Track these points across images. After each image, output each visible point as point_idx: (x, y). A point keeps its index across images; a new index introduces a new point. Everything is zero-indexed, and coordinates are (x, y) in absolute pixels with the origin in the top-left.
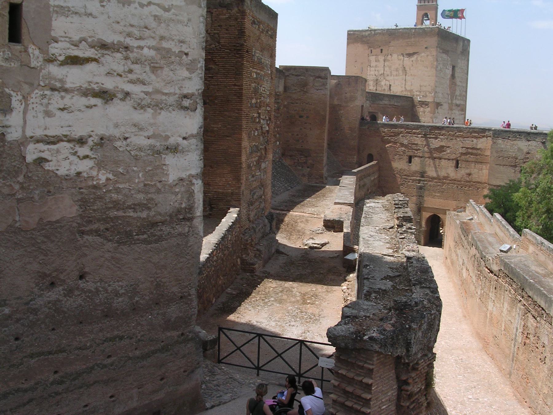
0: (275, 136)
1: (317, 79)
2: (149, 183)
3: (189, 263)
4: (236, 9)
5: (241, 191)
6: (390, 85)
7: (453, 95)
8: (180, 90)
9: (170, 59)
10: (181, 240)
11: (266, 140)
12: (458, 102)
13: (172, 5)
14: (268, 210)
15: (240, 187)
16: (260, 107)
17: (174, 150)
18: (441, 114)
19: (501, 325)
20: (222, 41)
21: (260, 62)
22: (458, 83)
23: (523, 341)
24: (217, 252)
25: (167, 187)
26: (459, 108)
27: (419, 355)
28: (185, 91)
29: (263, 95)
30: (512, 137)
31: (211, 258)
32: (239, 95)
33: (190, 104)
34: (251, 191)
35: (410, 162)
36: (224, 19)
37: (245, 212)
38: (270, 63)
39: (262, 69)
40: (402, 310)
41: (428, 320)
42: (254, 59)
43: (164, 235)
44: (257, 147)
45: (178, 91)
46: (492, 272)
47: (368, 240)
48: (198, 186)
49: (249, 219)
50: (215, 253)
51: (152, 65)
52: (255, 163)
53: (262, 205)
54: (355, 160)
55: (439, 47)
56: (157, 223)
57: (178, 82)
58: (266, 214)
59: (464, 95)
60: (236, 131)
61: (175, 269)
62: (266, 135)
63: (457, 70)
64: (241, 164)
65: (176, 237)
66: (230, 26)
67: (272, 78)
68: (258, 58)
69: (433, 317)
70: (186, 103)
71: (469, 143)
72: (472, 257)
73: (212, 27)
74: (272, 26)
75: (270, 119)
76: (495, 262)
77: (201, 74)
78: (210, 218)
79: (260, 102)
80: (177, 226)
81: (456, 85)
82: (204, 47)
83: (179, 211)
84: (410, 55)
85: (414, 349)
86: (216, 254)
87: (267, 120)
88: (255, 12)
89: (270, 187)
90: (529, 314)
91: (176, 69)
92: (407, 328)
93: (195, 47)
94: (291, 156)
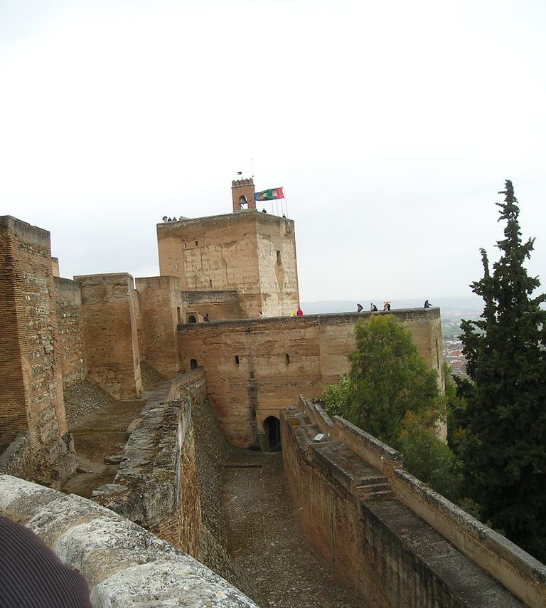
0: (76, 353)
7: (281, 284)
12: (288, 291)
26: (290, 297)
27: (158, 520)
35: (237, 362)
44: (41, 368)
49: (40, 440)
53: (56, 427)
55: (259, 233)
58: (61, 435)
64: (23, 387)
71: (296, 334)
74: (44, 245)
75: (54, 339)
81: (283, 271)
84: (228, 245)
85: (150, 515)
89: (63, 406)
94: (98, 373)
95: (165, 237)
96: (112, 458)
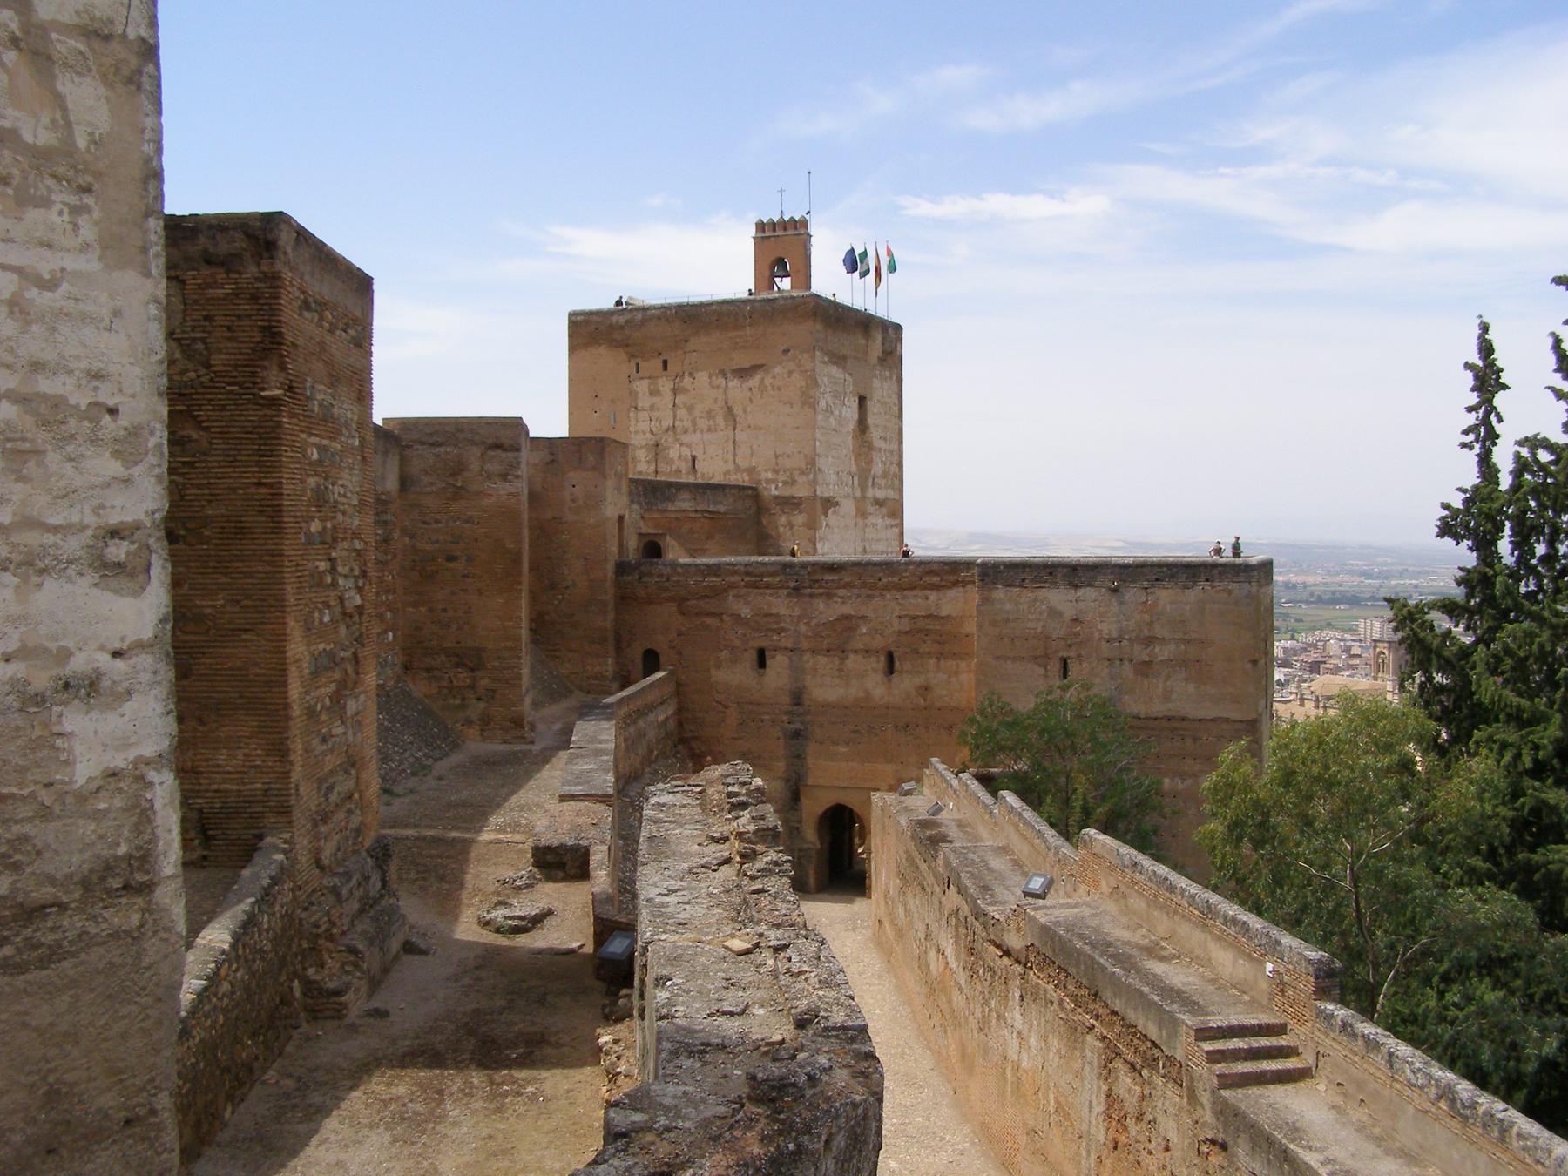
0: (381, 617)
1: (491, 453)
2: (15, 790)
3: (148, 1017)
4: (252, 270)
5: (293, 786)
6: (694, 459)
7: (864, 477)
8: (98, 515)
9: (63, 427)
10: (119, 952)
11: (357, 634)
12: (880, 494)
13: (63, 270)
14: (372, 833)
15: (286, 775)
16: (335, 540)
17: (85, 689)
18: (836, 530)
19: (1046, 1098)
20: (217, 360)
21: (327, 418)
22: (878, 443)
23: (1110, 1138)
24: (230, 966)
25: (69, 800)
26: (884, 510)
28: (114, 519)
29: (341, 507)
30: (1032, 581)
31: (213, 989)
32: (275, 513)
33: (128, 553)
34: (320, 781)
35: (762, 662)
36: (219, 299)
37: (305, 842)
38: (356, 418)
39: (335, 435)
40: (773, 1100)
41: (847, 1123)
42: (310, 407)
43: (66, 943)
44: (331, 655)
45: (90, 519)
46: (1007, 953)
47: (662, 905)
48: (164, 790)
49: (318, 863)
50: (223, 972)
51: (9, 445)
52: (327, 701)
53: (355, 821)
54: (610, 668)
55: (822, 350)
56: (44, 907)
57: (91, 492)
58: (367, 844)
59: (895, 476)
60: (268, 615)
61: (106, 1040)
62: (356, 618)
63: (873, 408)
64: (287, 706)
65: (104, 943)
66: (239, 317)
67: (364, 458)
68: (320, 405)
69: (860, 1110)
70: (118, 551)
71: (918, 603)
72: (950, 915)
73: (185, 321)
74: (358, 314)
75: (364, 573)
76: (1013, 926)
77: (159, 466)
78: (204, 867)
79: (334, 528)
80: (105, 913)
81: (871, 448)
82: (163, 389)
83: (108, 868)
84: (743, 373)
86: (228, 975)
87: (355, 577)
88: (307, 277)
89: (373, 765)
90: (1118, 1064)
91: (83, 456)
92: (792, 1153)
93: (138, 389)
94: (428, 670)
95: (587, 345)
96: (499, 914)
